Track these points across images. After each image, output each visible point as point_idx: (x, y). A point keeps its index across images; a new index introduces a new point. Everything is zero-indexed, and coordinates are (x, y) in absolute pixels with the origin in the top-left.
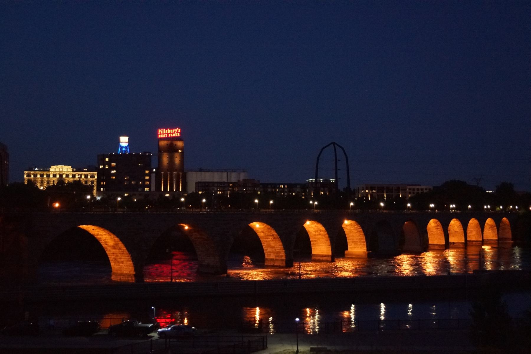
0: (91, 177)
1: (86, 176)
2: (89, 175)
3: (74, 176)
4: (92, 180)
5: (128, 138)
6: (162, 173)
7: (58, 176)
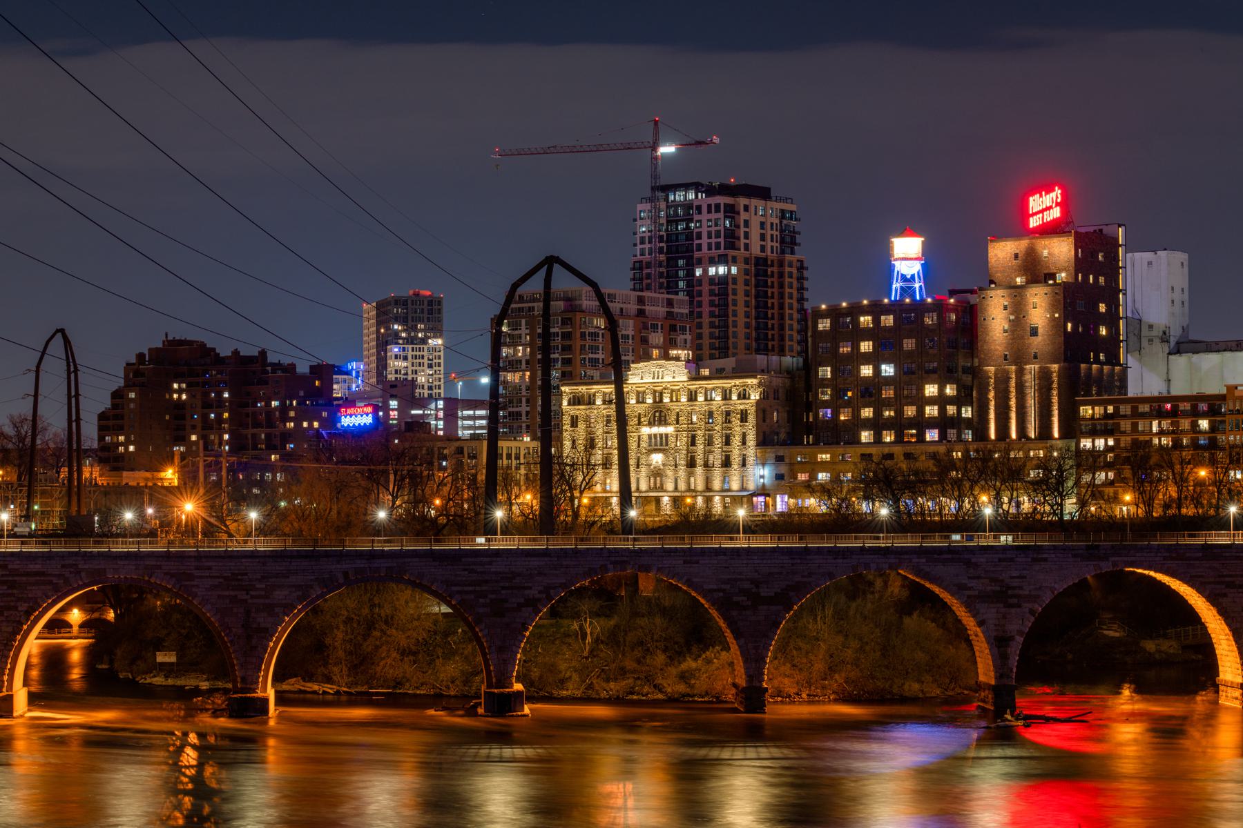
0: (739, 398)
1: (726, 396)
2: (734, 389)
3: (692, 397)
4: (742, 407)
5: (923, 242)
6: (987, 372)
7: (649, 400)
